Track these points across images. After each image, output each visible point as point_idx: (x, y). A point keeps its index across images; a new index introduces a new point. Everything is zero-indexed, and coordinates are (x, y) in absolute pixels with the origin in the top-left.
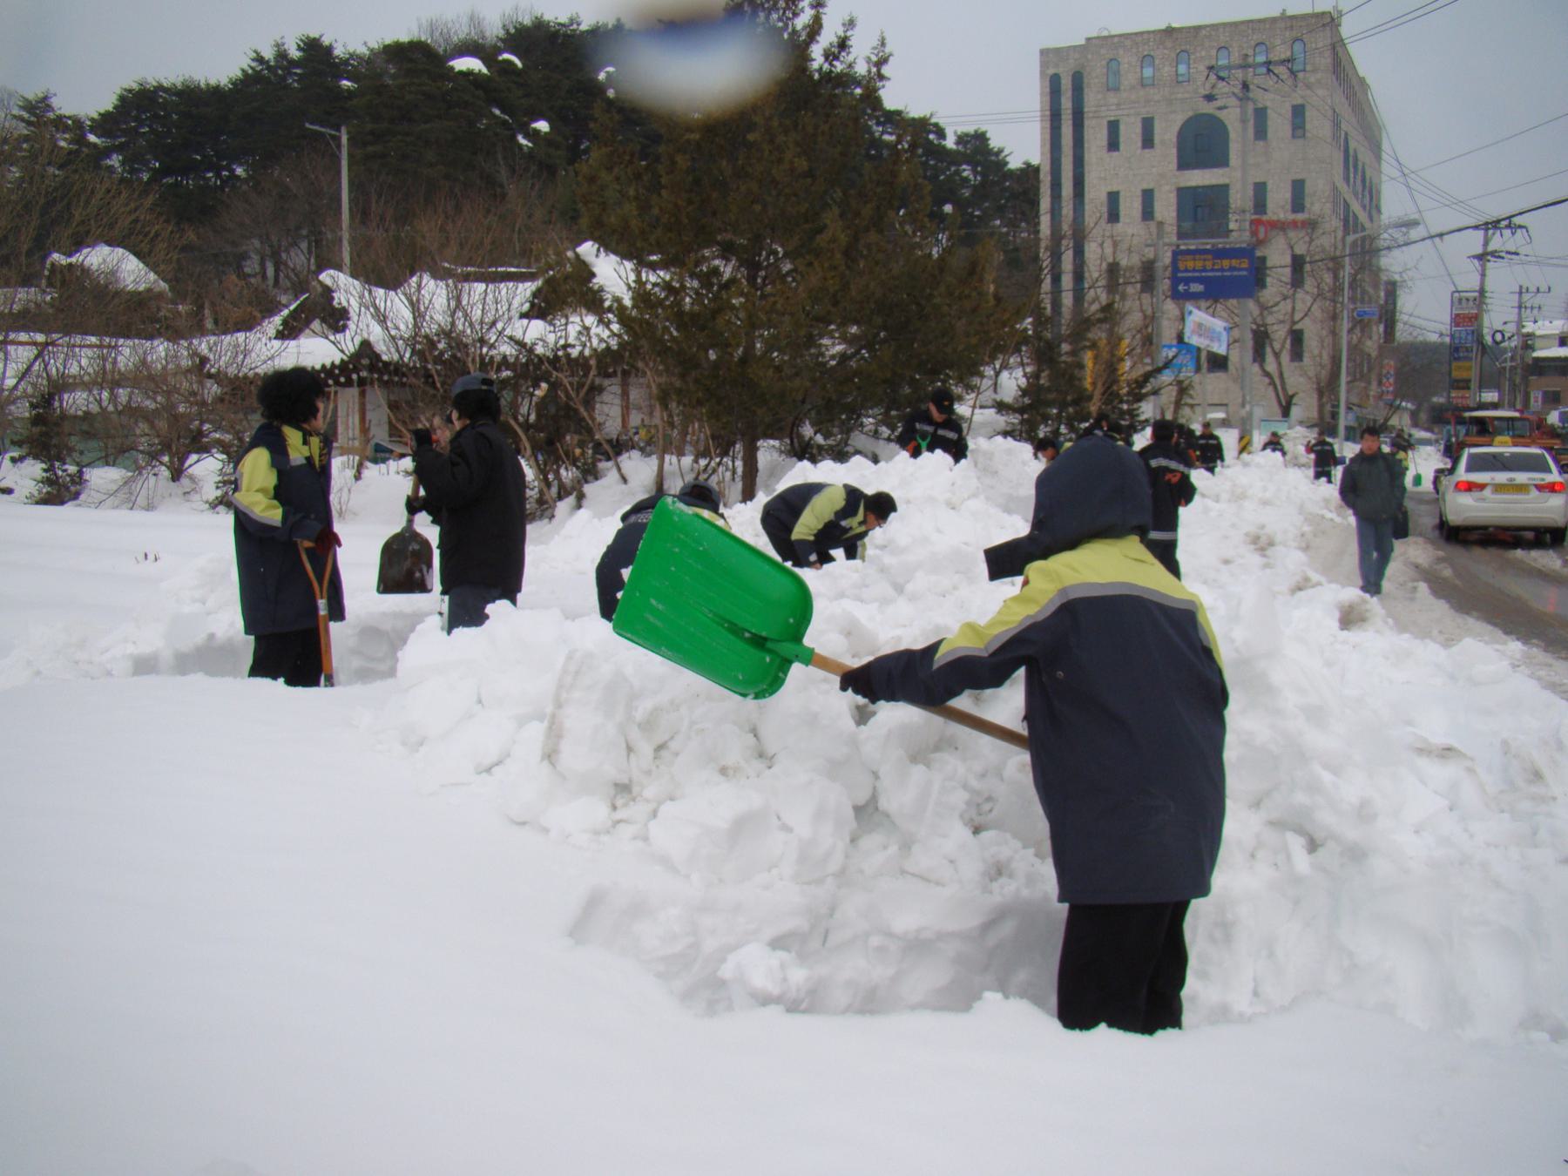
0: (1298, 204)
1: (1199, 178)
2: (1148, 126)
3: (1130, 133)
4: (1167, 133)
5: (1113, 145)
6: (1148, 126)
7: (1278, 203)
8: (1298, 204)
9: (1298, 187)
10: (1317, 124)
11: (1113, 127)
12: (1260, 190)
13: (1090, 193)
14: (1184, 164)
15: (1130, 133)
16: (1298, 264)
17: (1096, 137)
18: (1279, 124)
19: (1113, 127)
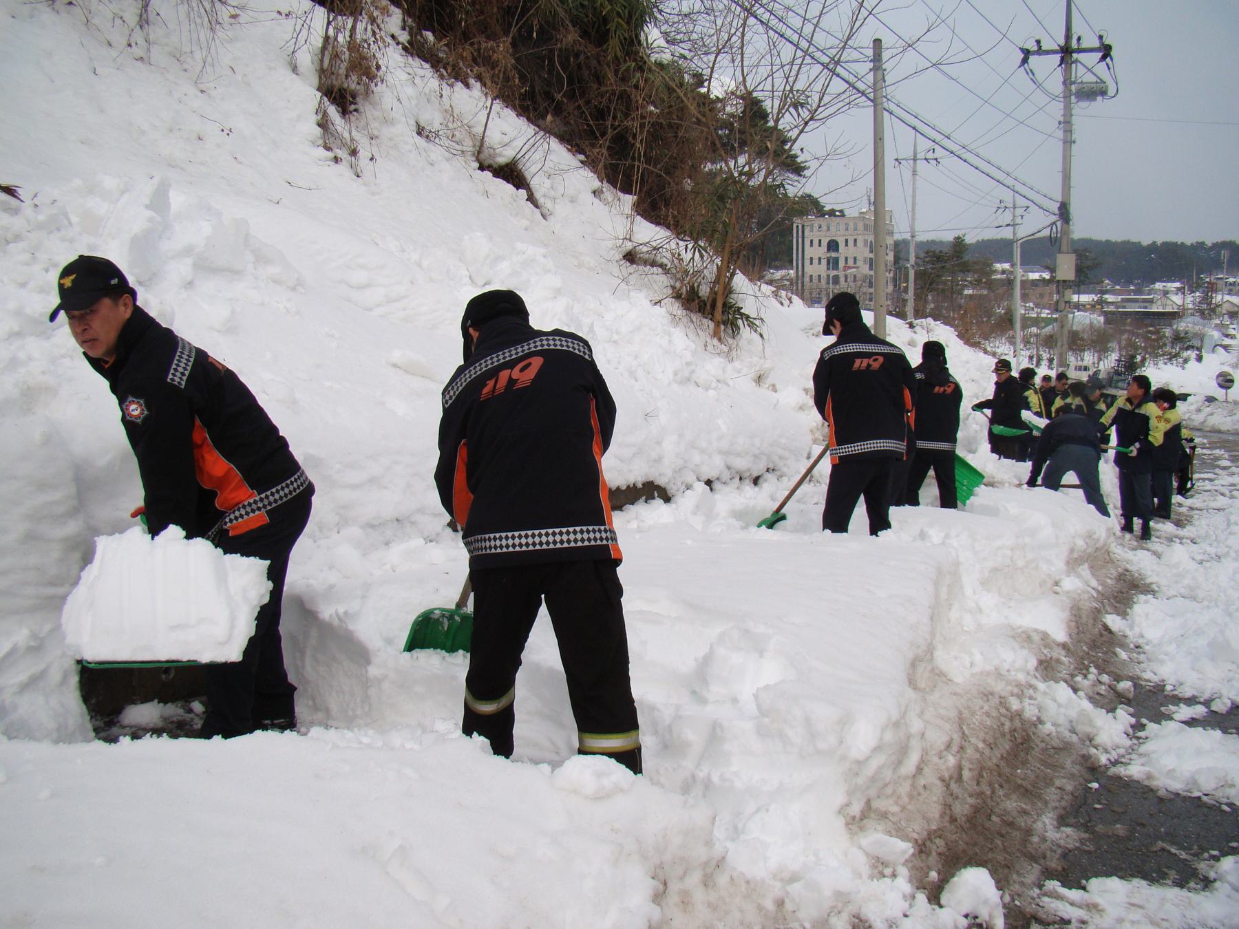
0: (855, 263)
1: (834, 255)
2: (820, 241)
3: (816, 242)
4: (825, 243)
5: (811, 245)
6: (820, 241)
7: (851, 263)
8: (855, 263)
9: (855, 259)
10: (860, 243)
11: (812, 241)
12: (846, 259)
13: (805, 257)
14: (829, 250)
15: (816, 242)
16: (855, 276)
17: (807, 243)
18: (851, 243)
19: (812, 241)
